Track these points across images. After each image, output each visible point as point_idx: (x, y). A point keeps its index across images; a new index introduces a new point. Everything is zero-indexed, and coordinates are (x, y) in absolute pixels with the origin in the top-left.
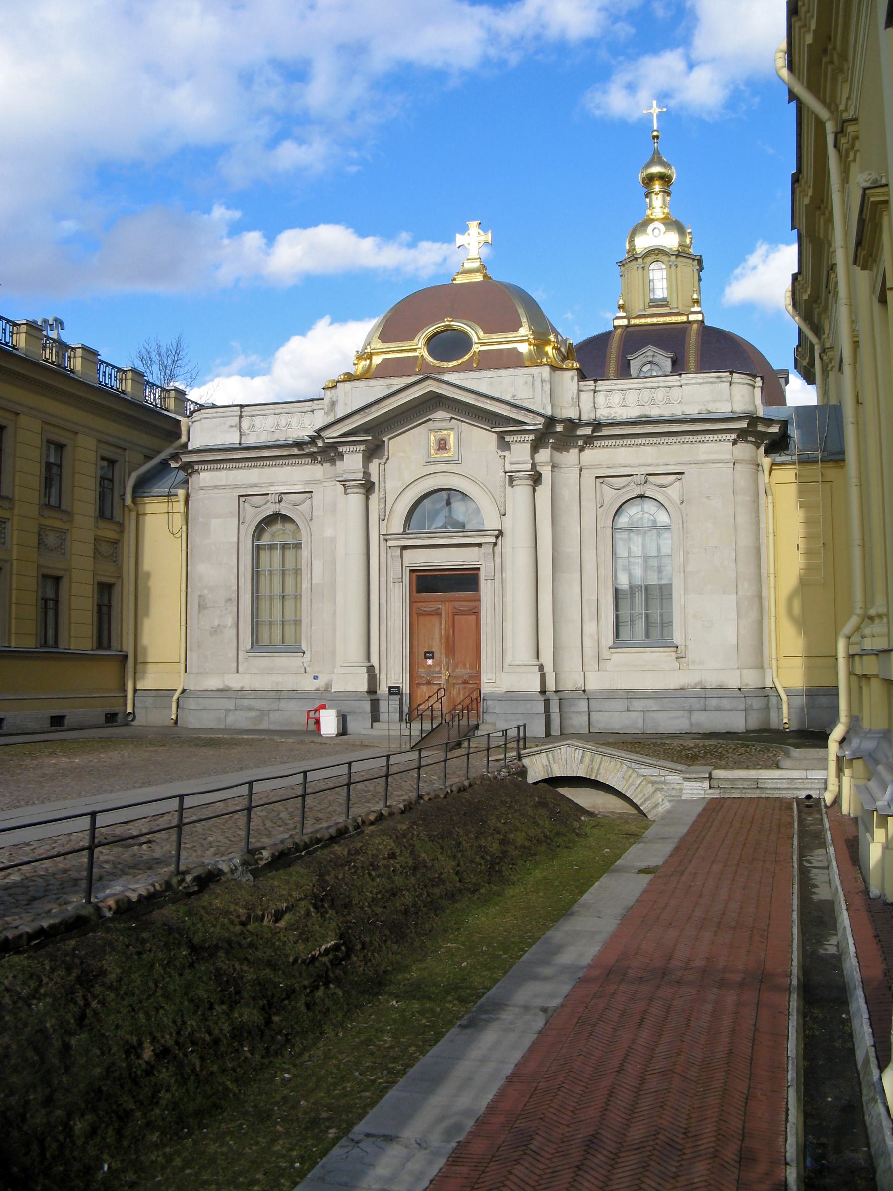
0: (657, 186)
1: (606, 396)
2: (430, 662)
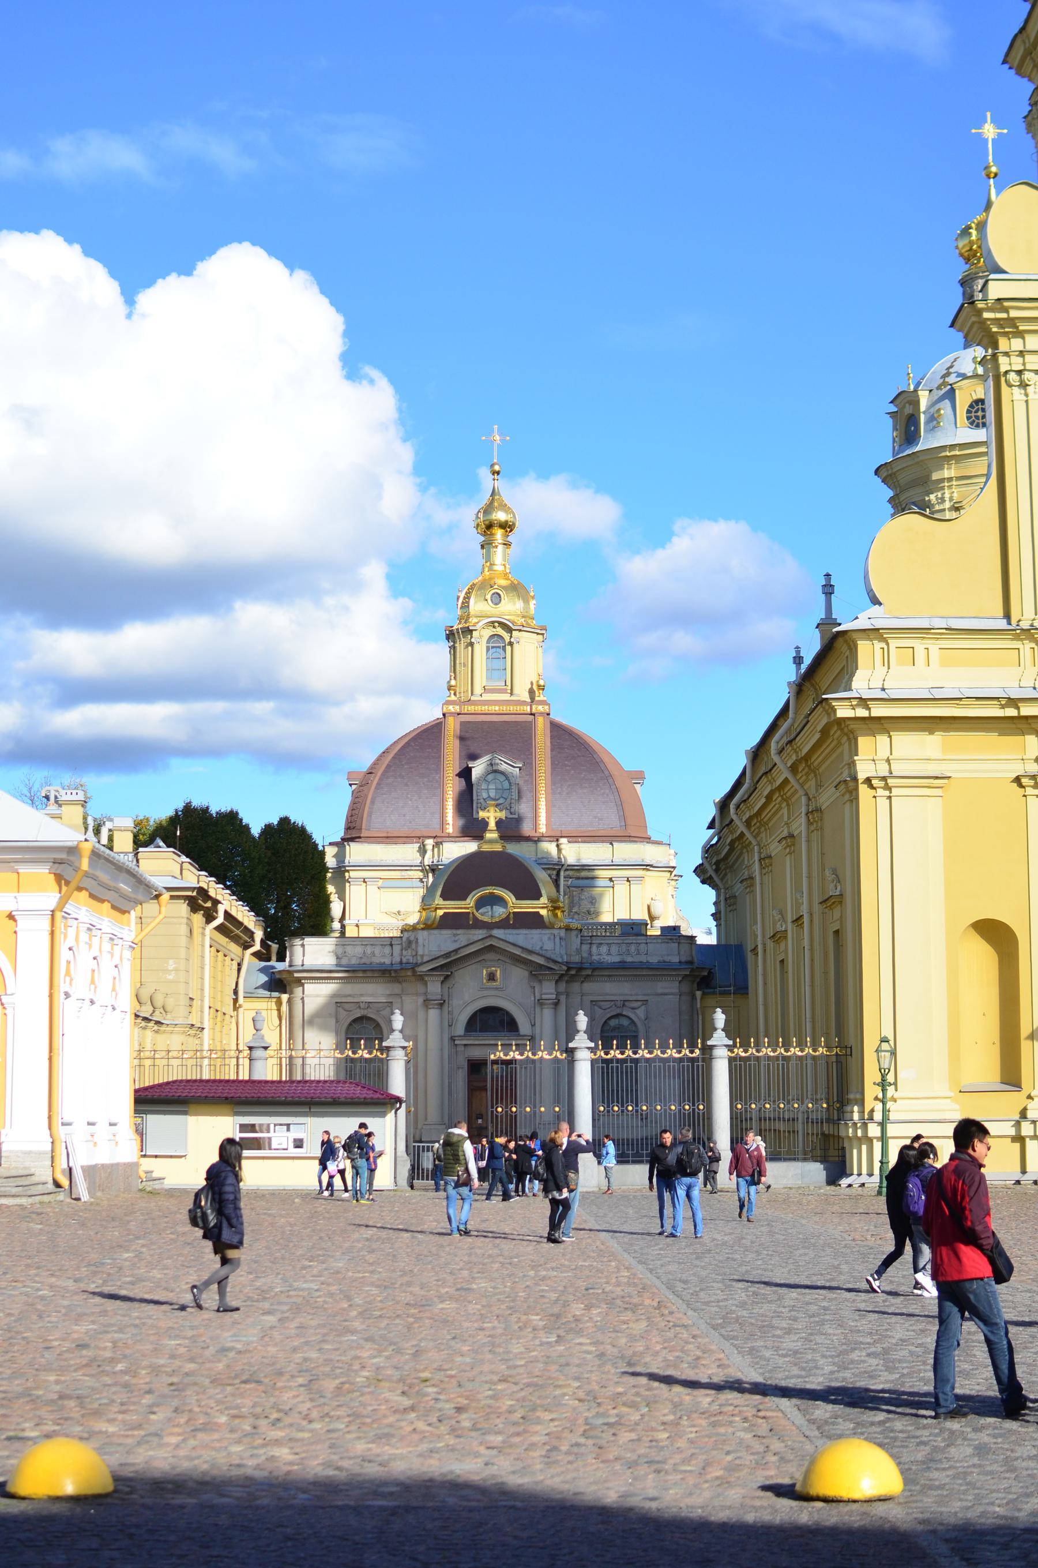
0: (499, 533)
1: (598, 947)
2: (480, 1121)
